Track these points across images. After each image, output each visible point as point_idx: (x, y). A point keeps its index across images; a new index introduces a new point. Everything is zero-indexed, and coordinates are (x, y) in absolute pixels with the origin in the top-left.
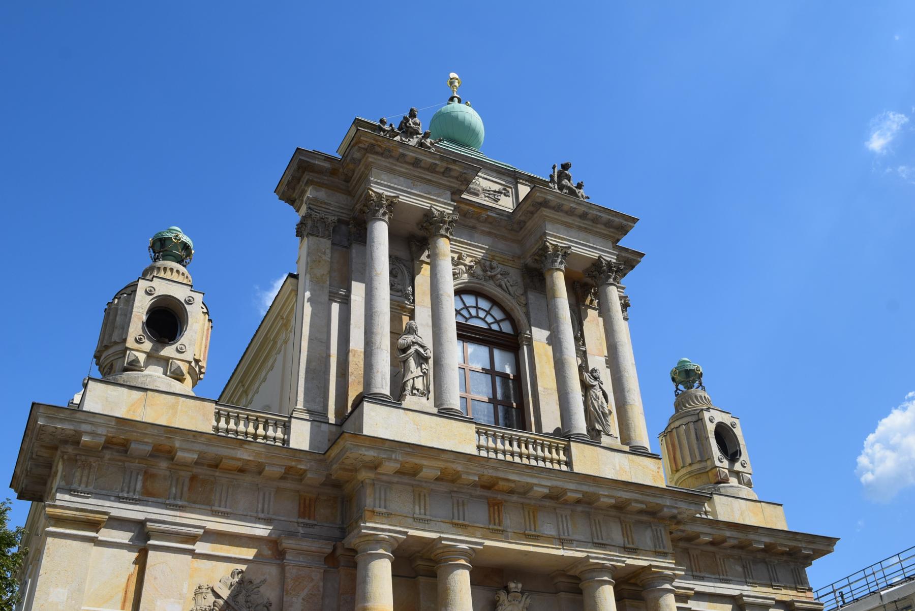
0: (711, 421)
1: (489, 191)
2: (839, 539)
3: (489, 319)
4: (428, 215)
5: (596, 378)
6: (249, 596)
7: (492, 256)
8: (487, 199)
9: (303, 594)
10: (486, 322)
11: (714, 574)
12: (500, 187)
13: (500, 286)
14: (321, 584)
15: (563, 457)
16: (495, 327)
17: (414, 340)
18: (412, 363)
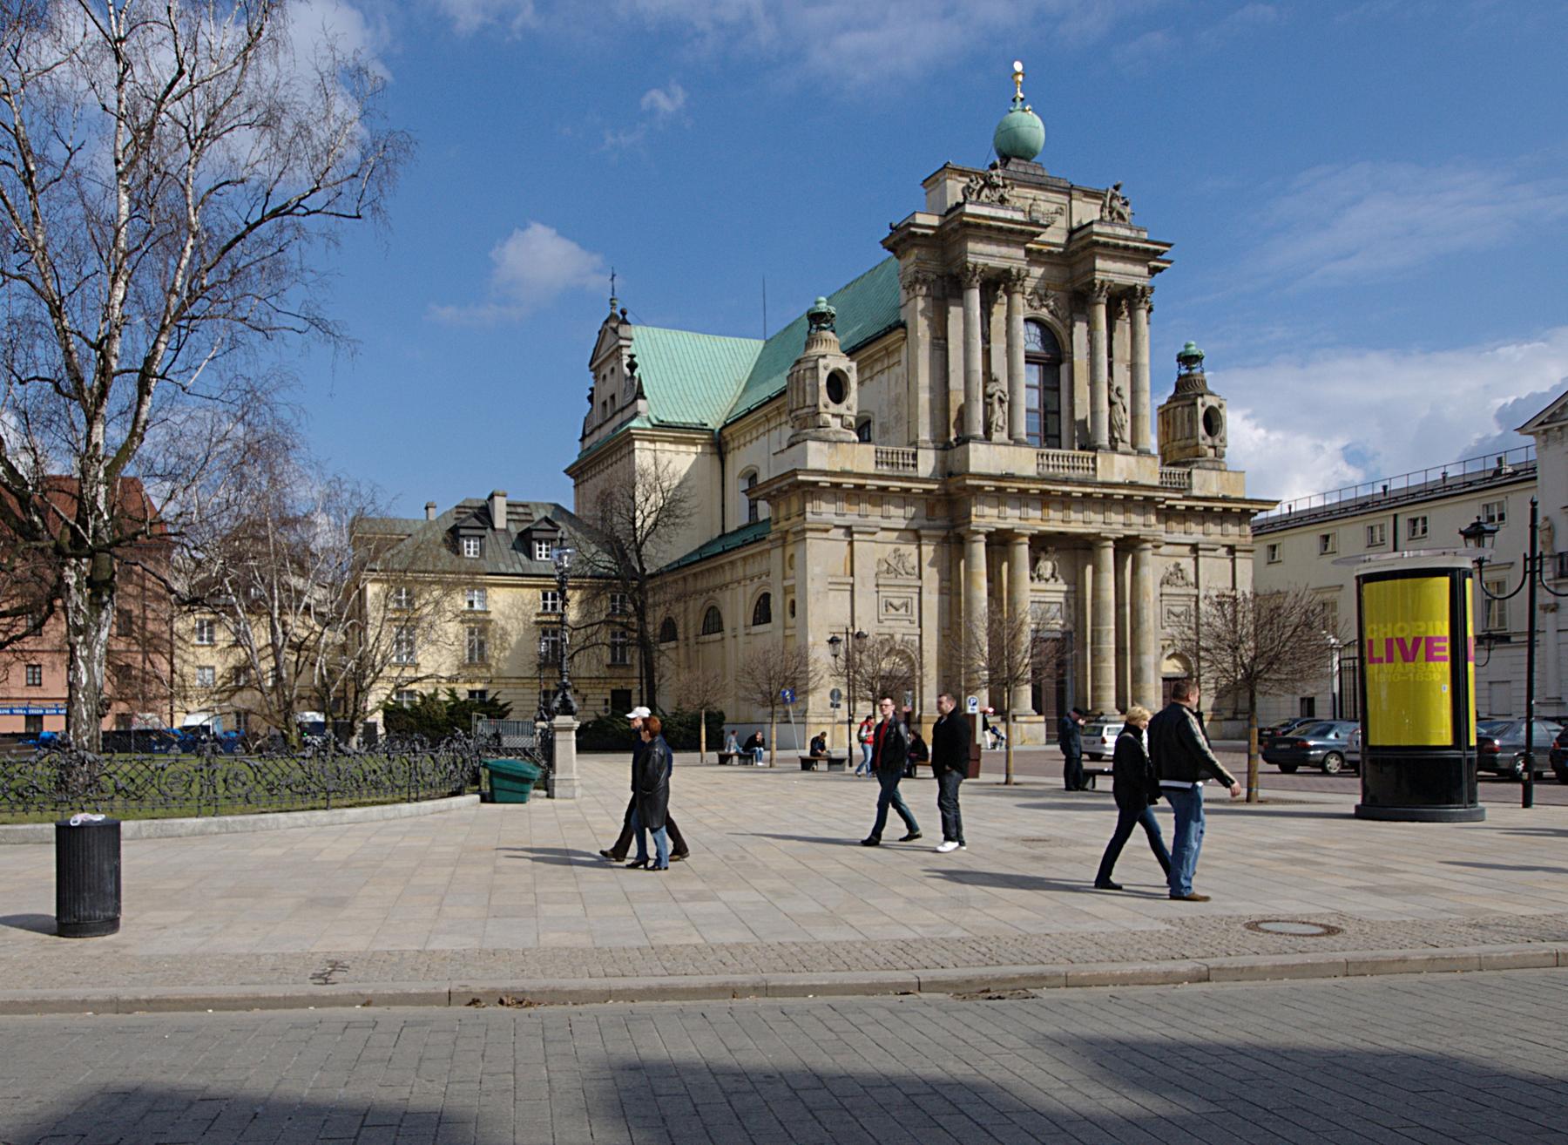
0: (1203, 405)
4: (1007, 271)
5: (1120, 396)
15: (1091, 465)
18: (996, 406)
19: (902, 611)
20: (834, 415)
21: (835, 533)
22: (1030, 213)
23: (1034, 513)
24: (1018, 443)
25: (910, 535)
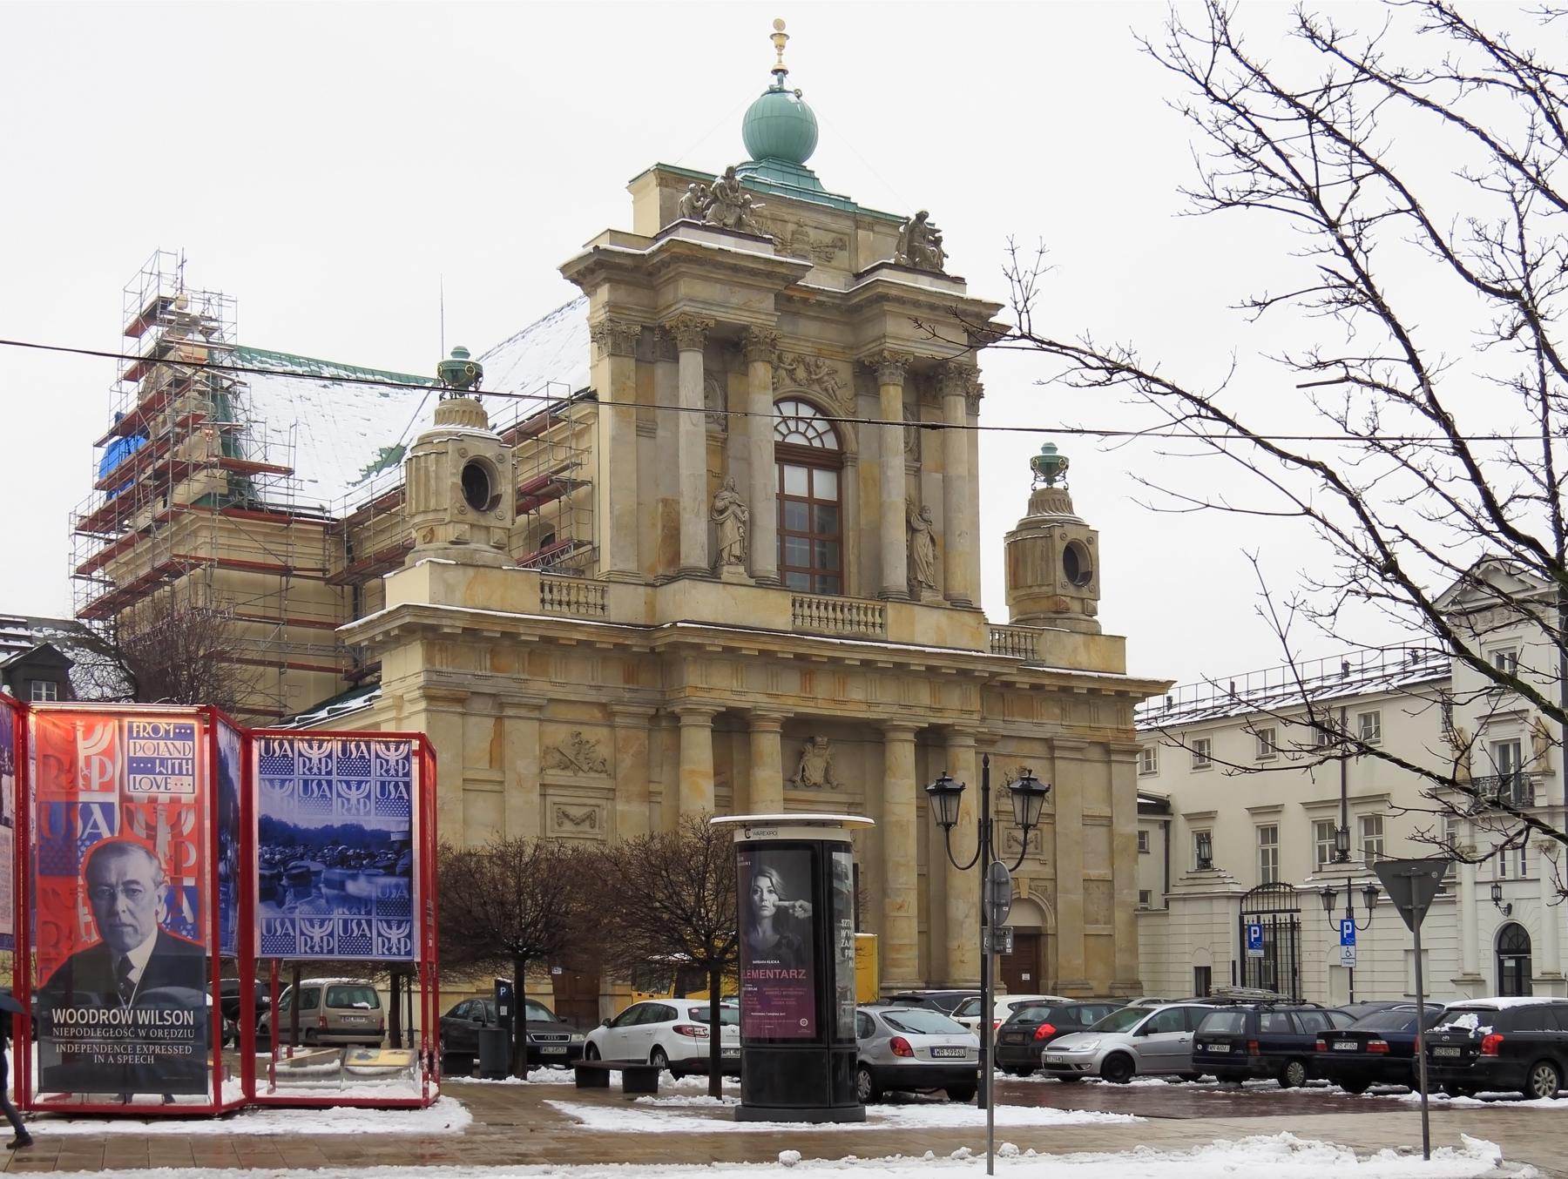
0: (1062, 538)
3: (811, 434)
7: (820, 349)
9: (631, 752)
10: (807, 437)
11: (1027, 718)
12: (834, 235)
13: (826, 390)
14: (647, 742)
16: (817, 443)
17: (731, 500)
19: (586, 827)
21: (477, 705)
24: (762, 583)
25: (597, 714)
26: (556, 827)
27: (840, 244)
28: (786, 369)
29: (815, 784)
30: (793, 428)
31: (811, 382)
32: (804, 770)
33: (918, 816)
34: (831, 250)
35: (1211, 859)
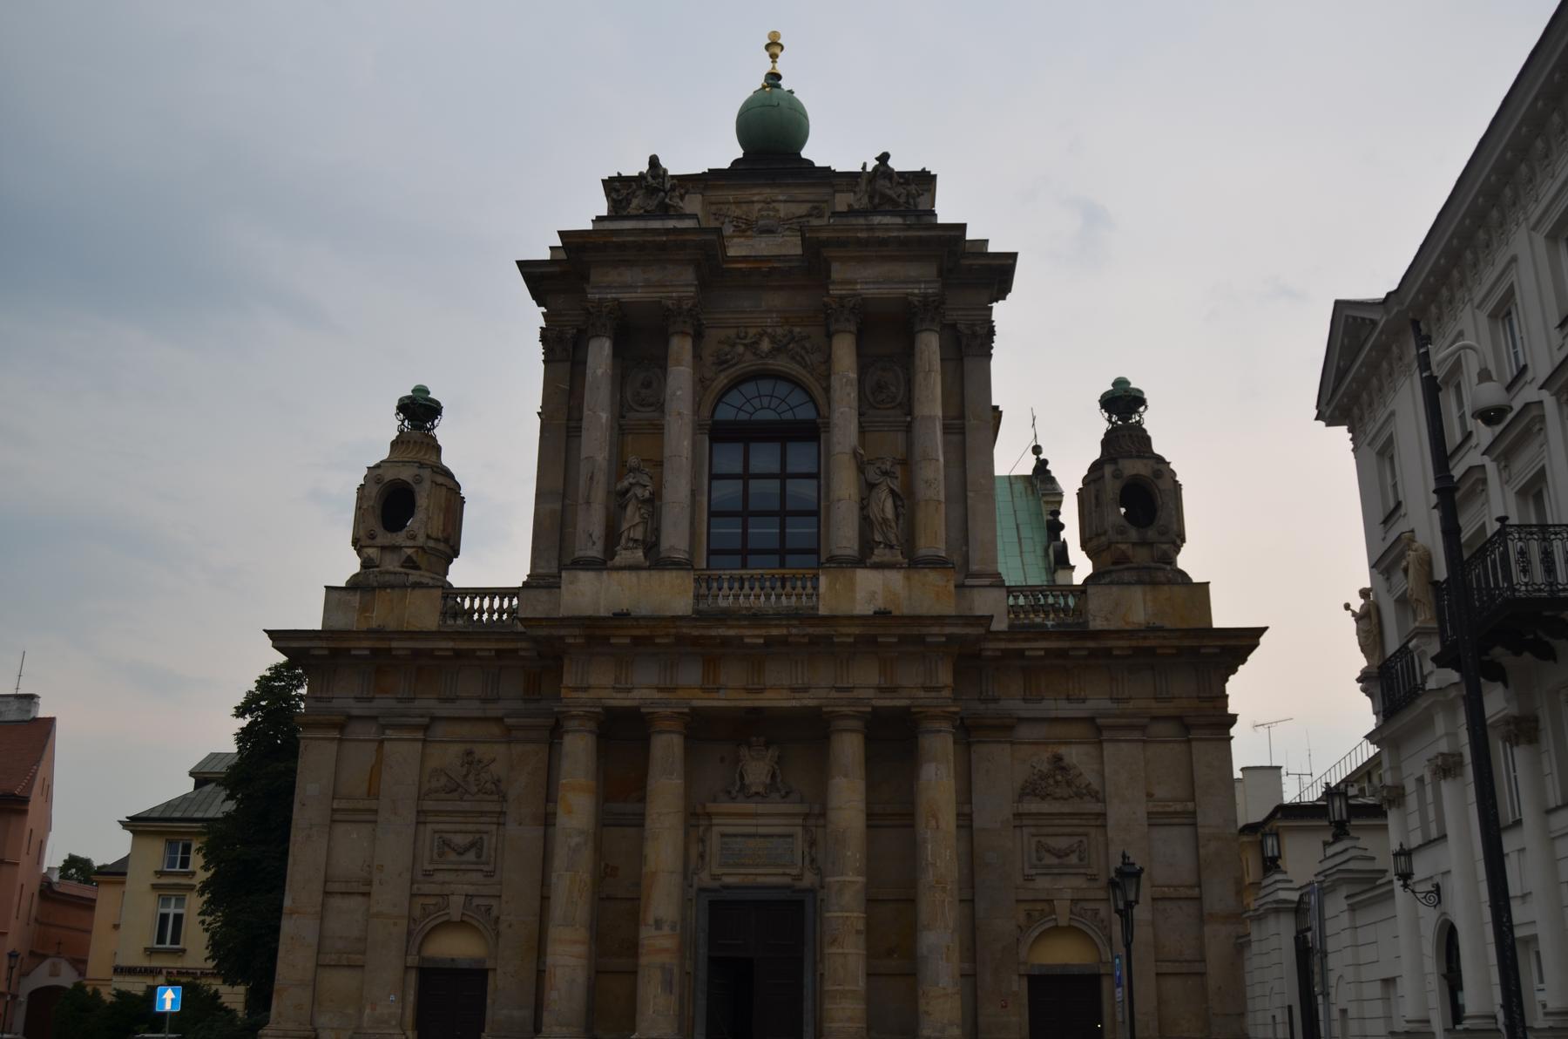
0: (1117, 475)
1: (791, 219)
2: (1265, 629)
6: (478, 774)
8: (787, 233)
12: (810, 205)
13: (793, 358)
16: (788, 416)
19: (471, 856)
20: (383, 548)
22: (757, 221)
23: (690, 675)
25: (495, 730)
26: (435, 857)
27: (817, 211)
28: (745, 345)
29: (757, 794)
30: (758, 405)
31: (777, 350)
32: (742, 777)
33: (958, 826)
34: (804, 219)
35: (1280, 857)
